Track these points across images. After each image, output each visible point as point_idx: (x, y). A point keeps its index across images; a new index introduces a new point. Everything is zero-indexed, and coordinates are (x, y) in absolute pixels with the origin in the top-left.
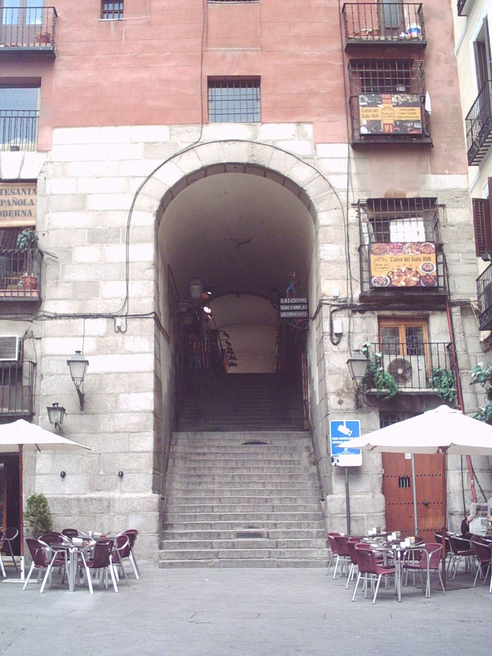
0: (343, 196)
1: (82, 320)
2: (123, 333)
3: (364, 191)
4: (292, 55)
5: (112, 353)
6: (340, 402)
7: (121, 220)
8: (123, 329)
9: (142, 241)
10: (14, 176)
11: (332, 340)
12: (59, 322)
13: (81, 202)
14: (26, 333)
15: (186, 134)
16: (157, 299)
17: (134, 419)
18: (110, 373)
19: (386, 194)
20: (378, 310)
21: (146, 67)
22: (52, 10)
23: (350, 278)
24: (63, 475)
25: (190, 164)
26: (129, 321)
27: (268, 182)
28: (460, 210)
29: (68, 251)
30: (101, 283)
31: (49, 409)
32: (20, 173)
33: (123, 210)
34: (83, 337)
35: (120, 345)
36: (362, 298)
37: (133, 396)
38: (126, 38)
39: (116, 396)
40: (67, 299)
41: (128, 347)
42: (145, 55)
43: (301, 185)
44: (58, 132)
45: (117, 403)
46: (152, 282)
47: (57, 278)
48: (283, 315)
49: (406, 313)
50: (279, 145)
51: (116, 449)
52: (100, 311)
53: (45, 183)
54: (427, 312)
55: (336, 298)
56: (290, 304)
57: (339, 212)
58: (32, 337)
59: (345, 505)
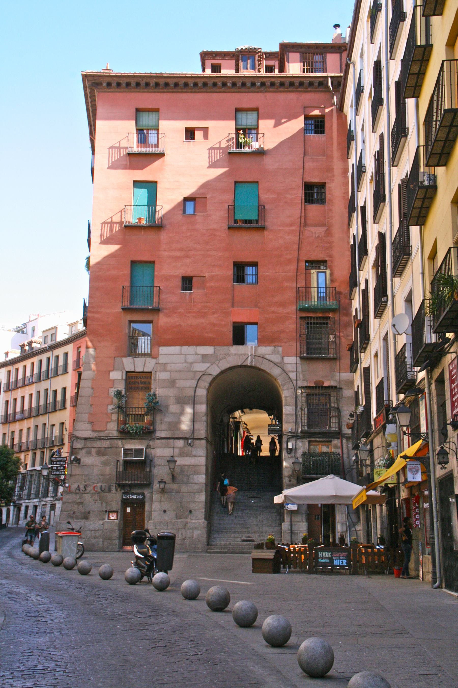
0: (295, 382)
1: (172, 440)
2: (192, 446)
3: (304, 380)
4: (273, 312)
5: (187, 456)
6: (290, 481)
7: (191, 393)
8: (192, 445)
9: (201, 403)
10: (141, 370)
11: (287, 452)
12: (163, 441)
13: (172, 383)
14: (147, 446)
15: (222, 350)
16: (207, 431)
17: (196, 487)
18: (185, 465)
19: (315, 383)
20: (309, 438)
21: (203, 317)
22: (158, 288)
23: (296, 422)
24: (165, 511)
25: (225, 365)
26: (194, 441)
28: (349, 390)
31: (159, 482)
32: (144, 368)
33: (192, 388)
34: (174, 448)
35: (190, 452)
36: (302, 432)
37: (196, 477)
38: (194, 302)
39: (188, 476)
40: (167, 430)
41: (194, 453)
42: (203, 311)
44: (161, 348)
45: (188, 479)
46: (205, 423)
47: (161, 420)
49: (321, 440)
51: (189, 501)
52: (181, 436)
53: (156, 374)
54: (331, 439)
55: (290, 432)
57: (293, 390)
58: (150, 447)
59: (290, 527)
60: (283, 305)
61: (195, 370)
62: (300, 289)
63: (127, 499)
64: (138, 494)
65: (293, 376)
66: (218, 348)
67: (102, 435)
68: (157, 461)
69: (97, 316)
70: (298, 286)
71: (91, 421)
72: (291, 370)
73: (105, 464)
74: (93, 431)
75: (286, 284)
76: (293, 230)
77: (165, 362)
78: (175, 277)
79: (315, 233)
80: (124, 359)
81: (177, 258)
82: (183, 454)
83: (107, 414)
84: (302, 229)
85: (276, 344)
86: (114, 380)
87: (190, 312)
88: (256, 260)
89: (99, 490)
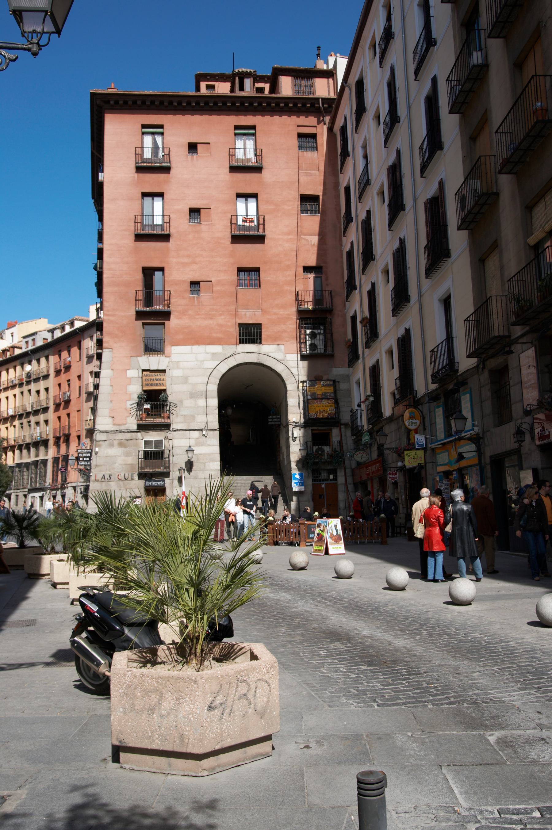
0: (297, 377)
1: (188, 432)
2: (206, 437)
5: (202, 446)
7: (203, 388)
9: (212, 397)
10: (155, 368)
13: (185, 380)
15: (231, 349)
20: (312, 426)
21: (211, 319)
22: (169, 292)
25: (232, 363)
27: (264, 369)
29: (181, 401)
30: (196, 416)
31: (179, 470)
37: (211, 464)
39: (204, 464)
41: (209, 443)
43: (279, 372)
48: (269, 423)
50: (270, 354)
55: (295, 422)
56: (272, 418)
57: (295, 385)
58: (168, 439)
60: (284, 307)
61: (205, 367)
62: (300, 293)
63: (150, 486)
64: (160, 481)
65: (295, 371)
66: (226, 347)
67: (123, 428)
68: (175, 451)
69: (112, 318)
70: (297, 290)
71: (112, 416)
72: (293, 366)
73: (127, 454)
74: (114, 424)
75: (287, 288)
76: (291, 239)
77: (177, 360)
78: (184, 281)
79: (311, 241)
80: (139, 358)
81: (185, 265)
82: (198, 444)
83: (126, 409)
84: (299, 238)
85: (279, 343)
86: (130, 378)
87: (199, 314)
88: (258, 266)
89: (123, 478)
